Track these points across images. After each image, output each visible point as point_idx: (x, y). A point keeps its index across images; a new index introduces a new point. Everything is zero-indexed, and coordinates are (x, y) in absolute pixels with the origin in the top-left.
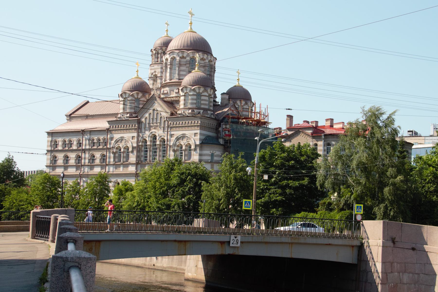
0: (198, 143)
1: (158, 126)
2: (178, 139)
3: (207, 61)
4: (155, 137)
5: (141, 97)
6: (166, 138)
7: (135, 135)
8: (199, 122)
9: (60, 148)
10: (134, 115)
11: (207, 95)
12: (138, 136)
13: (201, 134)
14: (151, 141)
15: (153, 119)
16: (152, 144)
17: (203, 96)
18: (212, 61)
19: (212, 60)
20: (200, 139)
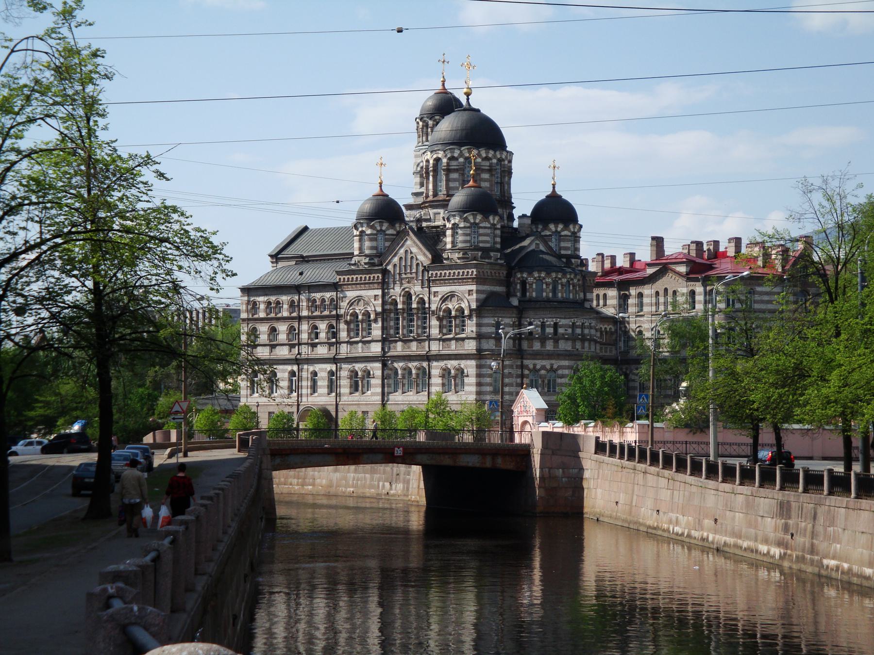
0: (474, 306)
1: (413, 278)
2: (444, 299)
3: (494, 161)
4: (408, 296)
5: (387, 229)
6: (426, 299)
7: (379, 292)
8: (475, 273)
9: (262, 315)
10: (376, 260)
11: (489, 225)
12: (384, 295)
13: (478, 292)
14: (404, 303)
15: (405, 266)
16: (405, 307)
17: (482, 228)
18: (503, 160)
19: (504, 157)
20: (477, 300)
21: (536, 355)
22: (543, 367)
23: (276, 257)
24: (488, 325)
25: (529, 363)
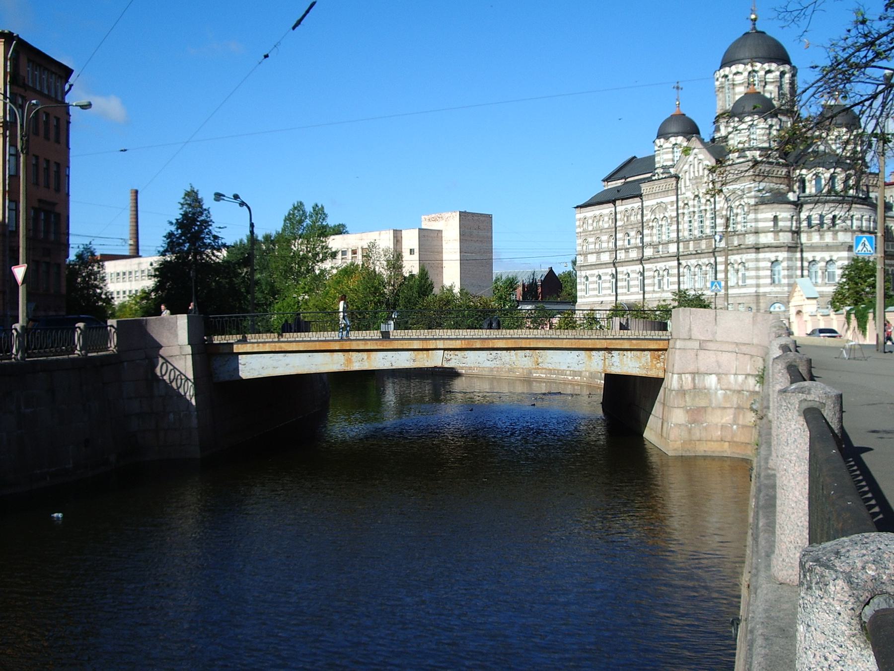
7: (674, 198)
15: (694, 172)
21: (813, 248)
22: (823, 259)
23: (608, 179)
24: (765, 220)
25: (808, 256)
